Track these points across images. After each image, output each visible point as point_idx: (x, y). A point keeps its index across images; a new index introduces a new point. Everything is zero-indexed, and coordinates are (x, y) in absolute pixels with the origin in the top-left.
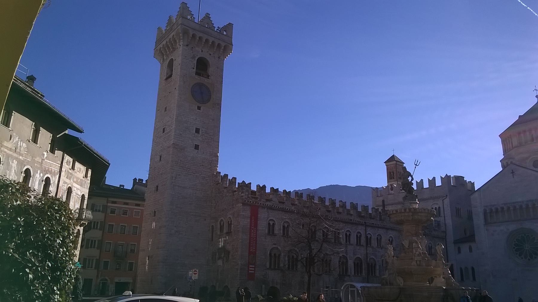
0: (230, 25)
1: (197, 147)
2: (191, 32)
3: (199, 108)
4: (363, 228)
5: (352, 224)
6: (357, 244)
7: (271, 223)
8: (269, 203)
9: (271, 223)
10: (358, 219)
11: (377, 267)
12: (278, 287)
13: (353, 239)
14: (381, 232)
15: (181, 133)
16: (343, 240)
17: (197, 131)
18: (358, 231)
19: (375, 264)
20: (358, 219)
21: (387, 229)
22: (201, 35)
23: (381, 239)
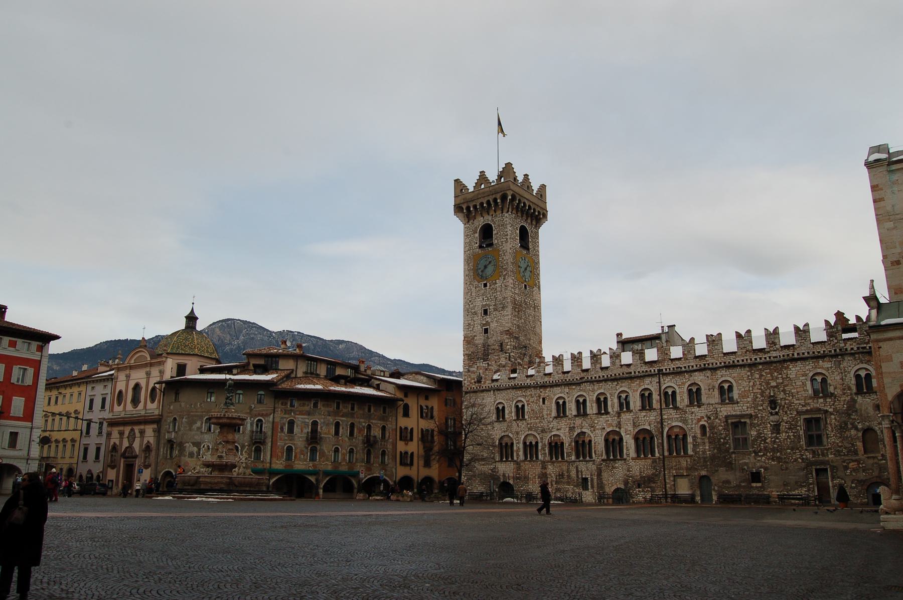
0: (509, 165)
3: (485, 285)
4: (656, 379)
5: (631, 378)
6: (643, 408)
7: (500, 407)
8: (496, 384)
9: (500, 407)
10: (645, 368)
11: (690, 440)
12: (511, 482)
14: (698, 378)
16: (613, 407)
17: (486, 312)
18: (643, 387)
19: (685, 436)
20: (645, 368)
21: (715, 369)
23: (699, 390)
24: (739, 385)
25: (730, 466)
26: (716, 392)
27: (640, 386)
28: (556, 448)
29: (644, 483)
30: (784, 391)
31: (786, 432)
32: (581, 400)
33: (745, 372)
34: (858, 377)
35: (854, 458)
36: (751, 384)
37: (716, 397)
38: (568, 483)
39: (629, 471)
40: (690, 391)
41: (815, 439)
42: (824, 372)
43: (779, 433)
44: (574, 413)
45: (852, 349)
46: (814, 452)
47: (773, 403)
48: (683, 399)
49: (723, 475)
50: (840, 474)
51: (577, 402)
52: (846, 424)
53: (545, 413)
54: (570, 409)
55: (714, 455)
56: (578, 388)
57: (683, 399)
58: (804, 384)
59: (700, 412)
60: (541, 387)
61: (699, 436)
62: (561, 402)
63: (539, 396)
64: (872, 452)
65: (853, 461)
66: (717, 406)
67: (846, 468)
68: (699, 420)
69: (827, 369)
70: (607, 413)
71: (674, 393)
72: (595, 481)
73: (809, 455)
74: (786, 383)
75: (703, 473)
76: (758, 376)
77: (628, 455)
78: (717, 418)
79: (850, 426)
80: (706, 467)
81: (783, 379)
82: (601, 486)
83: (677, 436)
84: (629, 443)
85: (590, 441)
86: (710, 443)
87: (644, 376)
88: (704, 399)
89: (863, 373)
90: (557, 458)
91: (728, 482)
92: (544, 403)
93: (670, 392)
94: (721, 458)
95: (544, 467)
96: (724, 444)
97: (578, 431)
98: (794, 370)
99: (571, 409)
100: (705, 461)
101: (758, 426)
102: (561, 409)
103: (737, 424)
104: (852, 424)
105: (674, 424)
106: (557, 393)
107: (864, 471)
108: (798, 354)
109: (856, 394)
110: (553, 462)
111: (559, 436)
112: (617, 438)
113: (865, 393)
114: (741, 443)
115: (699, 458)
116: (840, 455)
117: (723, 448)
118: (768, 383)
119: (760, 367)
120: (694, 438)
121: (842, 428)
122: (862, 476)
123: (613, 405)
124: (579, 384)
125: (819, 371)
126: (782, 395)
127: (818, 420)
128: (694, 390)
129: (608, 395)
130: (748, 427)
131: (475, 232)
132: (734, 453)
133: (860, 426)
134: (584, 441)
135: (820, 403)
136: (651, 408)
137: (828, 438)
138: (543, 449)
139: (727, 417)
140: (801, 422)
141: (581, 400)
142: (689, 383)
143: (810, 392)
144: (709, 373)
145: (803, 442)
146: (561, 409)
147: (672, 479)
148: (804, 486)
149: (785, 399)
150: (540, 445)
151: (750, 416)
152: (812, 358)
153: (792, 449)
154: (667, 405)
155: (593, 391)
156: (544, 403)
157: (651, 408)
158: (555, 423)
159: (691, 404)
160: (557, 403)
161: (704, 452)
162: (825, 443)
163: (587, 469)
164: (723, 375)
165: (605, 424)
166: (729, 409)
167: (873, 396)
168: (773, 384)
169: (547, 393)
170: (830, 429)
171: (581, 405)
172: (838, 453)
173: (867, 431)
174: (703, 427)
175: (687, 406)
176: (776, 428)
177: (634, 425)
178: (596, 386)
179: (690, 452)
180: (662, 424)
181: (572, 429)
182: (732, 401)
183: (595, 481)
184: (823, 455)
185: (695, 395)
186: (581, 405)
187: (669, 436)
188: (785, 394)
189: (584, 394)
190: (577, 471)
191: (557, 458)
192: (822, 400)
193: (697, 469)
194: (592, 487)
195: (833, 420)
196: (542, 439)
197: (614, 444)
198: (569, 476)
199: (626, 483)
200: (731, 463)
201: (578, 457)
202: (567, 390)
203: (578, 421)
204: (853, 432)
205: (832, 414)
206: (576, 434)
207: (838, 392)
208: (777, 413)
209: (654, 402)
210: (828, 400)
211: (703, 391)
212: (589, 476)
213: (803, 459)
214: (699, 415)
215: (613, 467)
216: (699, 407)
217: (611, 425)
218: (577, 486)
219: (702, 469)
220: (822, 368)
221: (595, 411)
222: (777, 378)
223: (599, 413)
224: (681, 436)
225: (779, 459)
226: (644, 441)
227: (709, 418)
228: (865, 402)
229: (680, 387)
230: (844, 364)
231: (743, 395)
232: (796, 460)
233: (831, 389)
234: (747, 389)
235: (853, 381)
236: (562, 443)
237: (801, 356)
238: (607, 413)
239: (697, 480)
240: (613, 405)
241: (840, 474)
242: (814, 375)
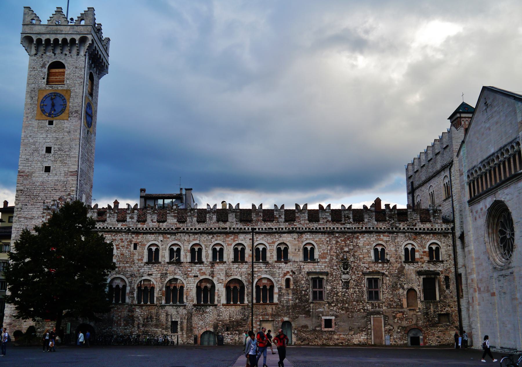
1: (47, 169)
2: (35, 38)
3: (51, 123)
4: (250, 236)
5: (227, 233)
6: (235, 261)
11: (276, 290)
13: (229, 254)
14: (287, 239)
15: (28, 157)
17: (48, 150)
18: (237, 242)
19: (272, 287)
20: (240, 226)
21: (302, 233)
22: (48, 36)
23: (286, 249)
24: (319, 248)
25: (308, 313)
26: (301, 254)
27: (234, 241)
28: (146, 292)
29: (233, 328)
30: (354, 256)
31: (354, 288)
32: (175, 248)
33: (324, 238)
34: (406, 250)
35: (400, 310)
36: (329, 248)
37: (300, 257)
38: (157, 326)
39: (219, 316)
40: (279, 250)
41: (374, 295)
42: (383, 243)
43: (348, 288)
44: (167, 260)
45: (404, 229)
46: (373, 305)
47: (346, 264)
48: (272, 256)
49: (302, 320)
50: (390, 322)
51: (171, 250)
52: (396, 285)
53: (136, 257)
54: (163, 256)
55: (296, 304)
56: (173, 237)
57: (272, 256)
58: (369, 252)
59: (286, 267)
60: (133, 233)
61: (284, 287)
62: (154, 248)
63: (131, 241)
64: (411, 306)
65: (400, 312)
66: (301, 263)
67: (395, 317)
68: (285, 274)
69: (386, 242)
70: (201, 262)
71: (264, 250)
72: (185, 325)
73: (370, 308)
74: (356, 249)
75: (286, 319)
76: (334, 242)
77: (219, 301)
78: (300, 273)
79: (399, 286)
80: (289, 314)
81: (354, 246)
82: (190, 329)
83: (265, 287)
84: (221, 291)
85: (182, 288)
86: (293, 294)
87: (239, 233)
88: (290, 257)
89: (410, 247)
90: (145, 302)
91: (306, 327)
92: (135, 248)
93: (261, 248)
94: (301, 307)
95: (132, 311)
96: (305, 295)
97: (170, 277)
98: (362, 240)
99: (164, 256)
100: (288, 309)
101: (332, 282)
102: (153, 257)
103: (317, 281)
104: (400, 284)
105: (263, 276)
106: (151, 239)
107: (406, 320)
108: (366, 228)
109: (404, 262)
110: (142, 306)
111: (150, 281)
112: (209, 285)
113: (411, 262)
114: (318, 296)
115: (283, 306)
116: (391, 308)
117: (304, 298)
118: (342, 249)
119: (337, 235)
120: (280, 289)
121: (394, 287)
122: (405, 323)
123: (207, 255)
124: (174, 234)
125: (380, 242)
126: (352, 259)
127: (376, 280)
128: (282, 249)
129: (203, 246)
130: (324, 283)
131: (43, 66)
132: (312, 303)
133: (405, 287)
134: (175, 287)
135: (379, 267)
136: (243, 261)
137: (383, 294)
138: (132, 292)
139: (309, 273)
140: (365, 281)
141: (175, 248)
142: (279, 242)
143: (373, 258)
144: (295, 236)
145: (366, 296)
146: (153, 257)
147: (258, 323)
148: (365, 331)
149: (354, 262)
150: (128, 289)
151: (327, 274)
152: (376, 232)
153: (357, 302)
154: (258, 259)
155: (189, 241)
156: (135, 248)
157: (243, 261)
158: (146, 269)
159: (279, 260)
160: (150, 250)
161: (287, 302)
162: (381, 298)
163: (175, 313)
164: (308, 238)
165: (200, 271)
166: (310, 266)
167: (416, 265)
168: (346, 249)
169: (140, 238)
170: (385, 287)
171: (175, 254)
172: (390, 306)
173: (411, 291)
174: (288, 281)
175: (276, 262)
176: (346, 284)
177: (227, 275)
178: (192, 237)
179: (276, 300)
180: (253, 276)
181: (164, 275)
182: (313, 260)
183: (185, 325)
184: (379, 307)
185: (283, 254)
186: (175, 254)
187: (257, 287)
188: (354, 258)
189: (179, 243)
190: (167, 315)
191: (145, 302)
192: (380, 265)
193: (280, 316)
194: (182, 330)
195: (387, 280)
196: (131, 283)
197: (205, 292)
198: (158, 320)
199: (216, 326)
200: (309, 311)
201: (167, 301)
202: (161, 238)
203: (171, 268)
204: (401, 291)
205: (387, 276)
206: (167, 280)
207: (392, 260)
208: (348, 273)
209: (246, 256)
210: (385, 265)
211: (290, 250)
212: (179, 320)
213: (364, 310)
214: (285, 270)
215: (204, 312)
216: (286, 263)
217: (204, 273)
218: (166, 329)
219: (285, 316)
220: (382, 240)
221: (189, 260)
222: (349, 245)
223: (193, 262)
224: (268, 287)
225: (347, 309)
226: (235, 290)
227: (294, 273)
228: (410, 268)
229: (270, 244)
230: (398, 239)
231: (323, 256)
232: (359, 310)
233: (388, 257)
234: (326, 251)
235: (403, 253)
236: (153, 288)
237: (368, 230)
238: (201, 262)
239: (280, 324)
240: (207, 255)
241: (390, 322)
242: (376, 245)
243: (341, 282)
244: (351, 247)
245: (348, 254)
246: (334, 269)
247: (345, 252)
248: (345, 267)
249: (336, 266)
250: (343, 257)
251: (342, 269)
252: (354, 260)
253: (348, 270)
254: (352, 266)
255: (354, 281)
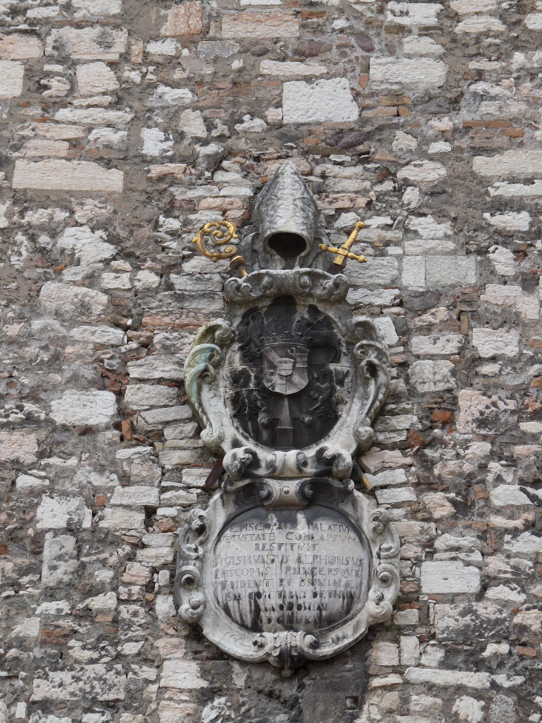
126: (428, 257)
188: (475, 242)
208: (327, 493)
243: (183, 673)
244: (420, 68)
245: (348, 179)
246: (56, 438)
247: (290, 138)
248: (286, 376)
249: (112, 380)
250: (251, 219)
251: (220, 423)
252: (463, 271)
253: (339, 444)
254: (432, 376)
255: (463, 650)
